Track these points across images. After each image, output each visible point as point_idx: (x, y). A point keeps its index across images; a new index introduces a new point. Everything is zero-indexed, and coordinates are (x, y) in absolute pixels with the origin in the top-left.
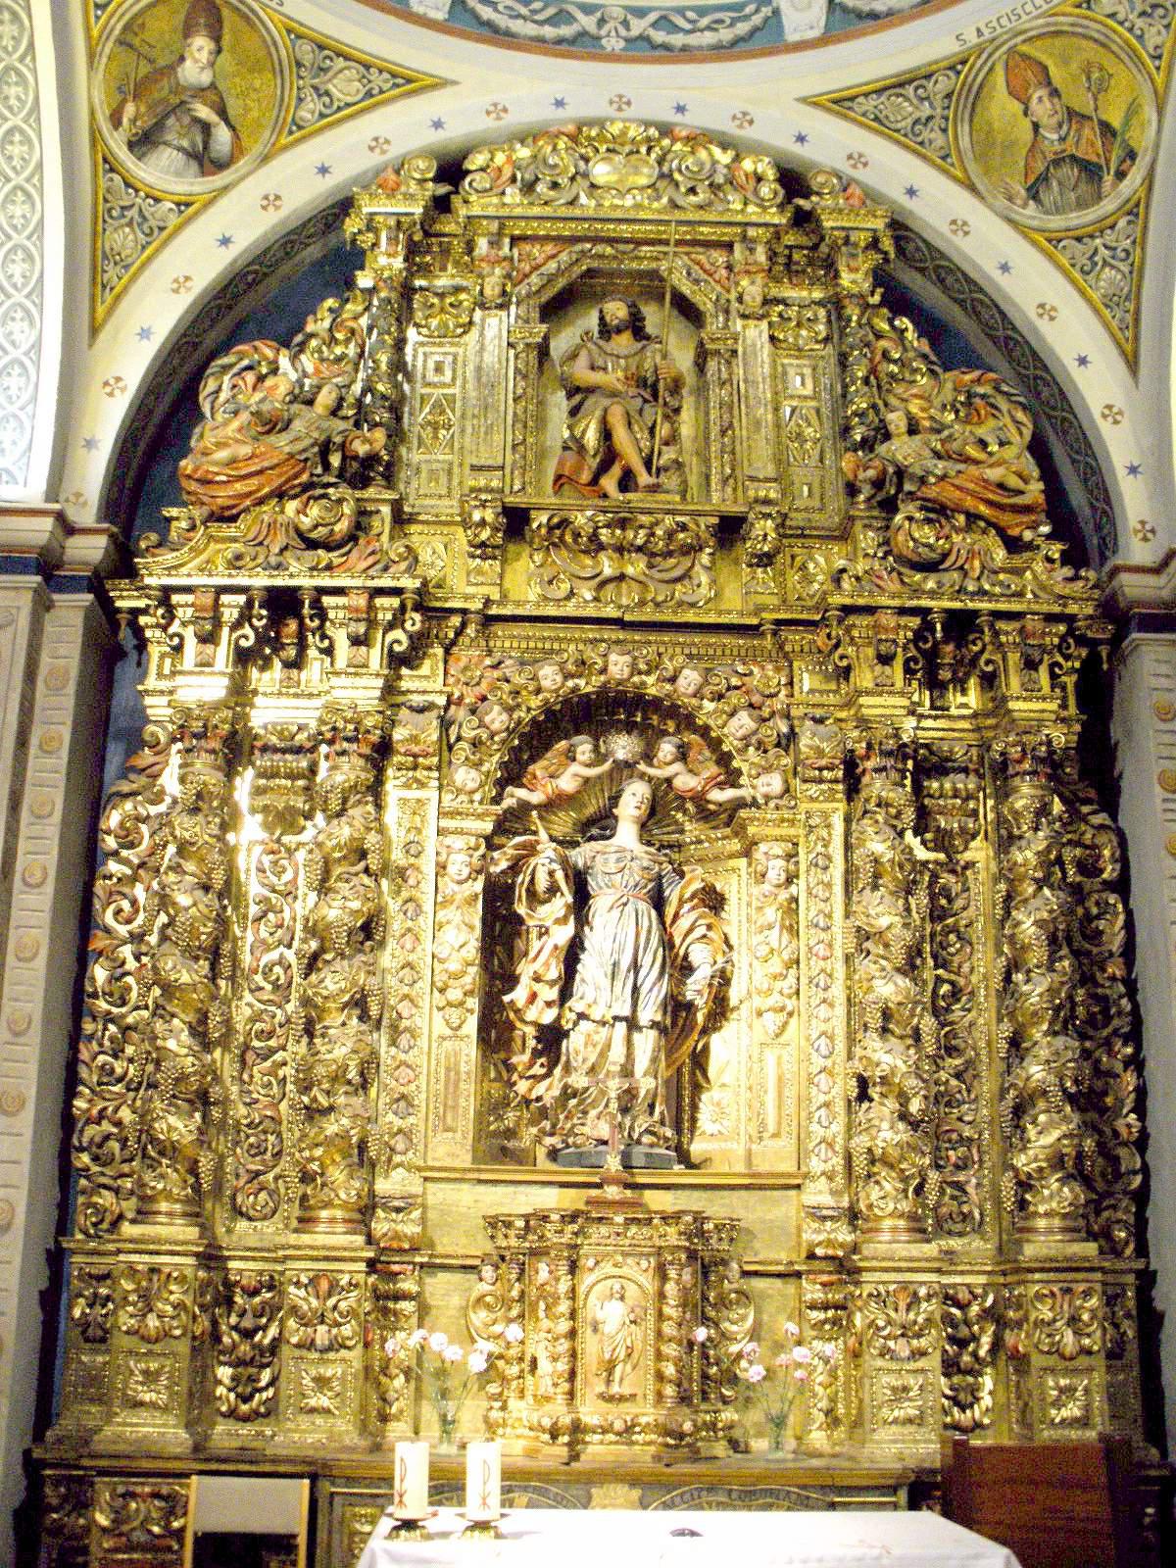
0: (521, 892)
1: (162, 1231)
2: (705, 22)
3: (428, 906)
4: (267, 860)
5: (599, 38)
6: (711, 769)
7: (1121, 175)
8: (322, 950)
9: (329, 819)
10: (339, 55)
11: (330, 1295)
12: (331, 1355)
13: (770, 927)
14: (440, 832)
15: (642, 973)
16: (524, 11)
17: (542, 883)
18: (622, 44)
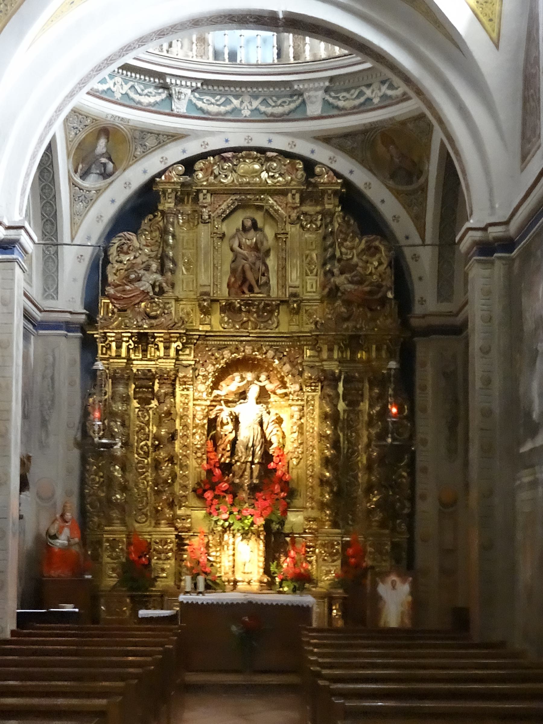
0: (218, 423)
1: (115, 528)
2: (279, 102)
3: (191, 428)
4: (140, 413)
5: (241, 110)
6: (277, 383)
7: (418, 178)
8: (159, 444)
9: (160, 403)
10: (148, 133)
11: (165, 545)
12: (166, 562)
13: (295, 432)
14: (194, 405)
15: (255, 448)
16: (213, 101)
17: (225, 421)
18: (249, 112)
